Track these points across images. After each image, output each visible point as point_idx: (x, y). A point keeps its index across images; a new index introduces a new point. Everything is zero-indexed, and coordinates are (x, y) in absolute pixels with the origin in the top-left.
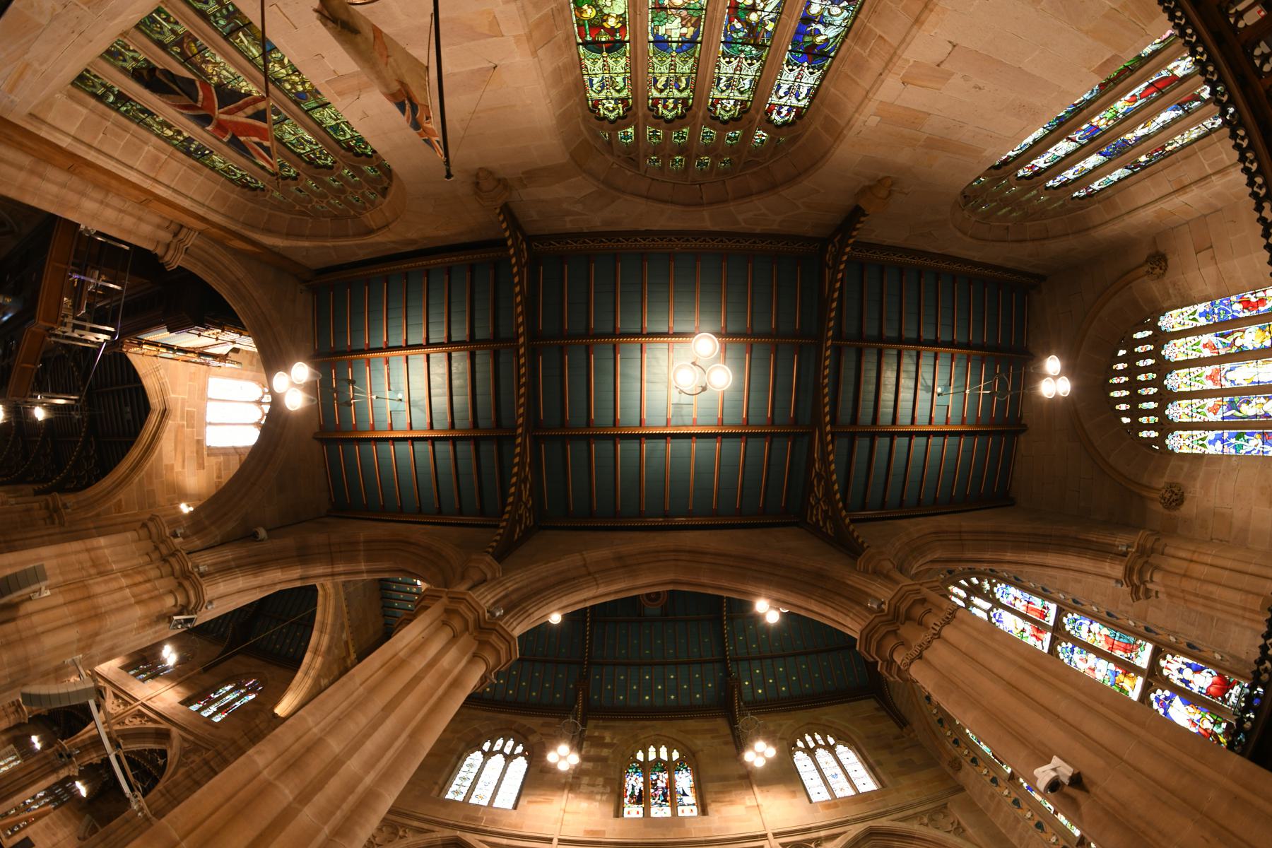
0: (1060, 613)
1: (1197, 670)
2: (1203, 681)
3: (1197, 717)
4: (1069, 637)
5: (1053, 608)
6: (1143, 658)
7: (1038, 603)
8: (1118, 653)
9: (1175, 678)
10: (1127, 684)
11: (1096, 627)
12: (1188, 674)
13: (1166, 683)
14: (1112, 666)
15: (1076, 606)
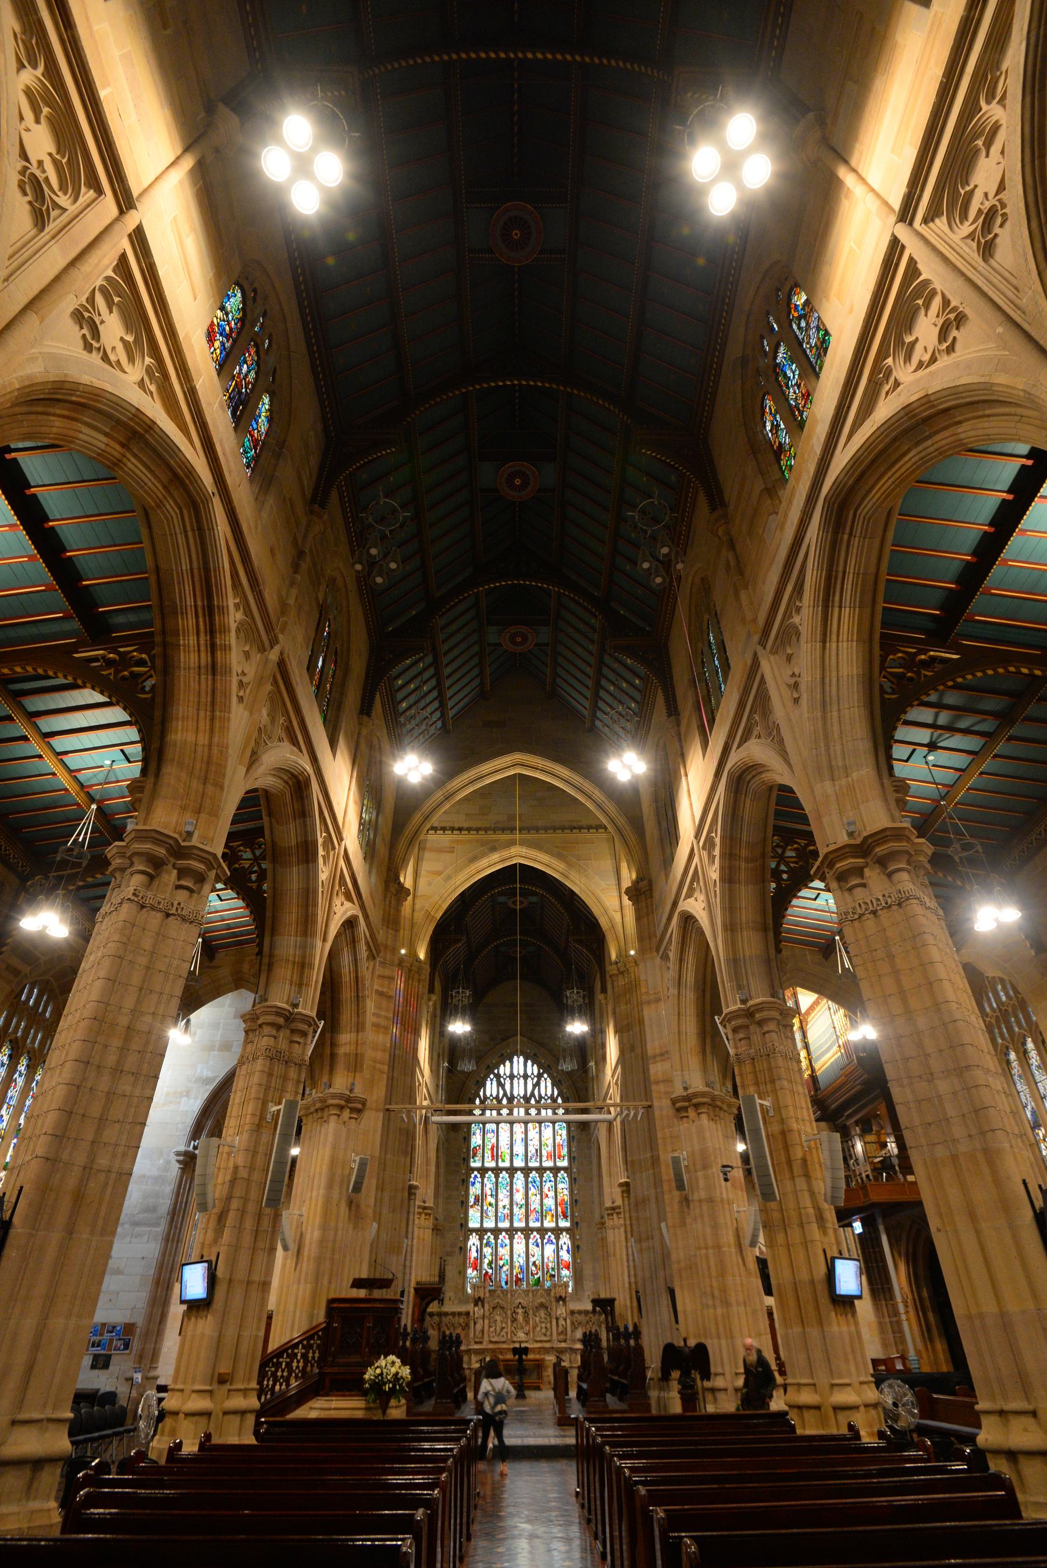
0: (565, 1169)
1: (568, 1251)
2: (566, 1256)
3: (551, 1259)
4: (555, 1176)
5: (564, 1163)
6: (564, 1224)
7: (564, 1151)
8: (559, 1209)
9: (561, 1242)
10: (549, 1218)
11: (566, 1192)
12: (565, 1247)
13: (558, 1238)
14: (553, 1207)
15: (573, 1181)
